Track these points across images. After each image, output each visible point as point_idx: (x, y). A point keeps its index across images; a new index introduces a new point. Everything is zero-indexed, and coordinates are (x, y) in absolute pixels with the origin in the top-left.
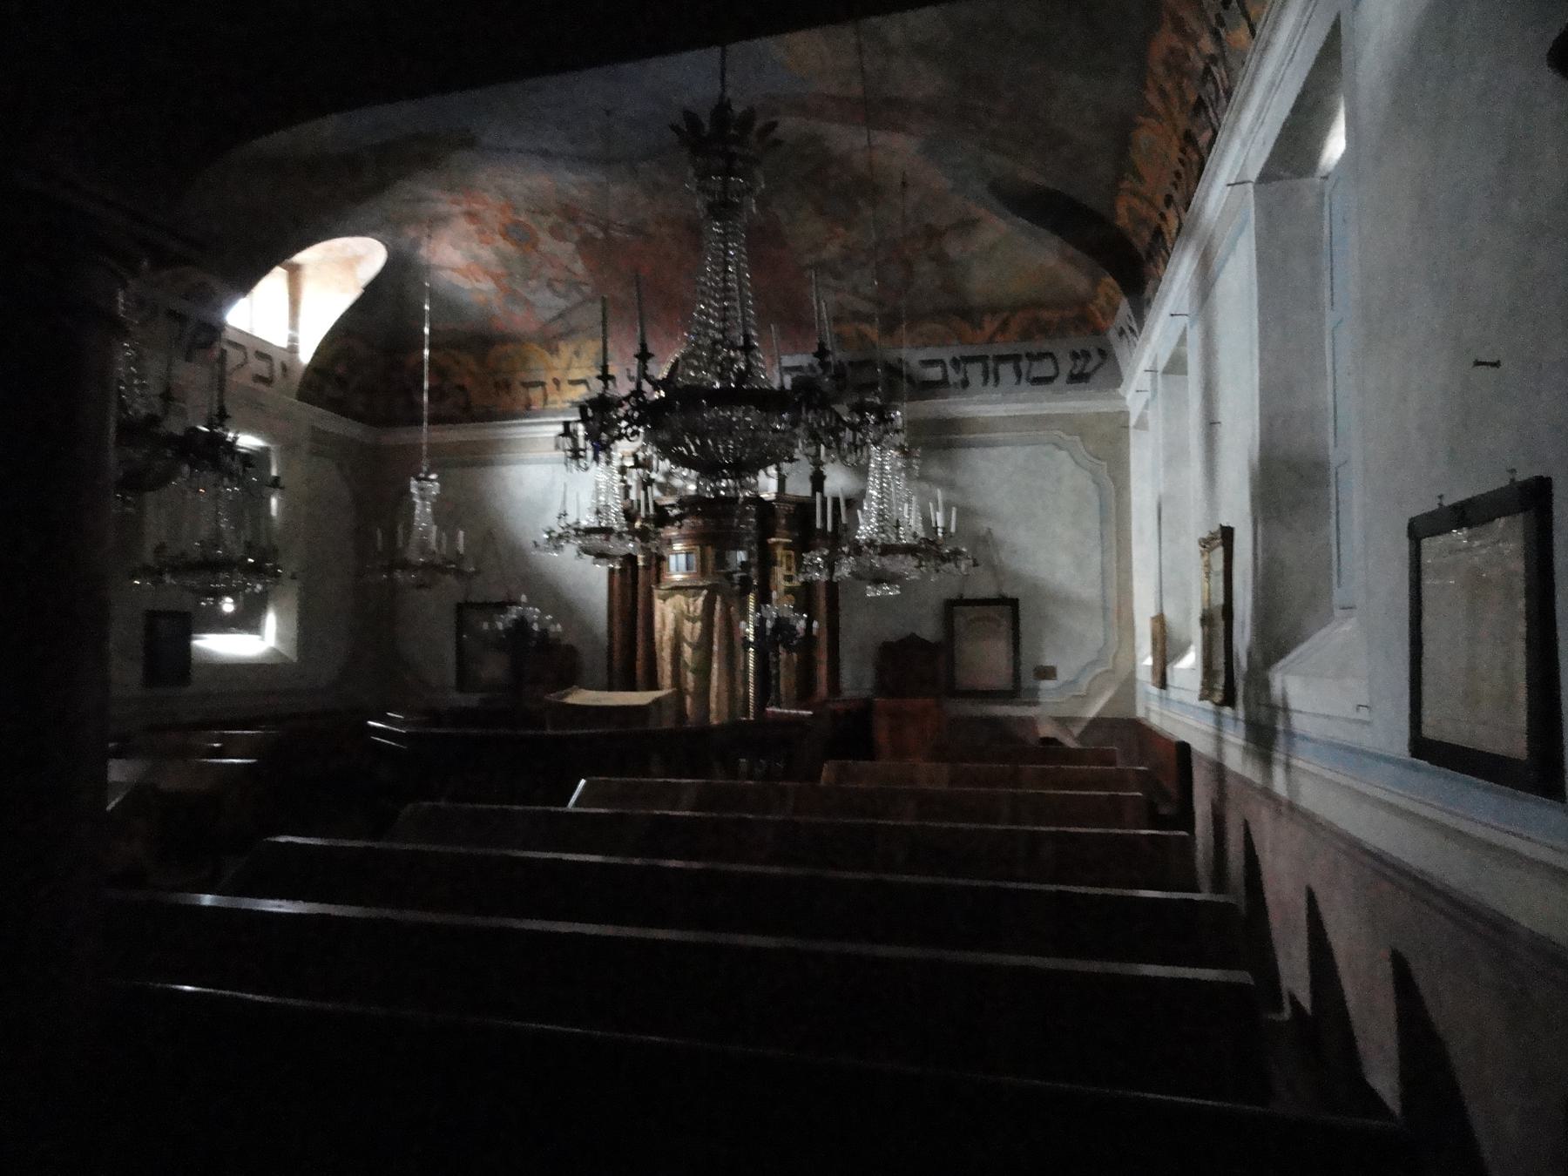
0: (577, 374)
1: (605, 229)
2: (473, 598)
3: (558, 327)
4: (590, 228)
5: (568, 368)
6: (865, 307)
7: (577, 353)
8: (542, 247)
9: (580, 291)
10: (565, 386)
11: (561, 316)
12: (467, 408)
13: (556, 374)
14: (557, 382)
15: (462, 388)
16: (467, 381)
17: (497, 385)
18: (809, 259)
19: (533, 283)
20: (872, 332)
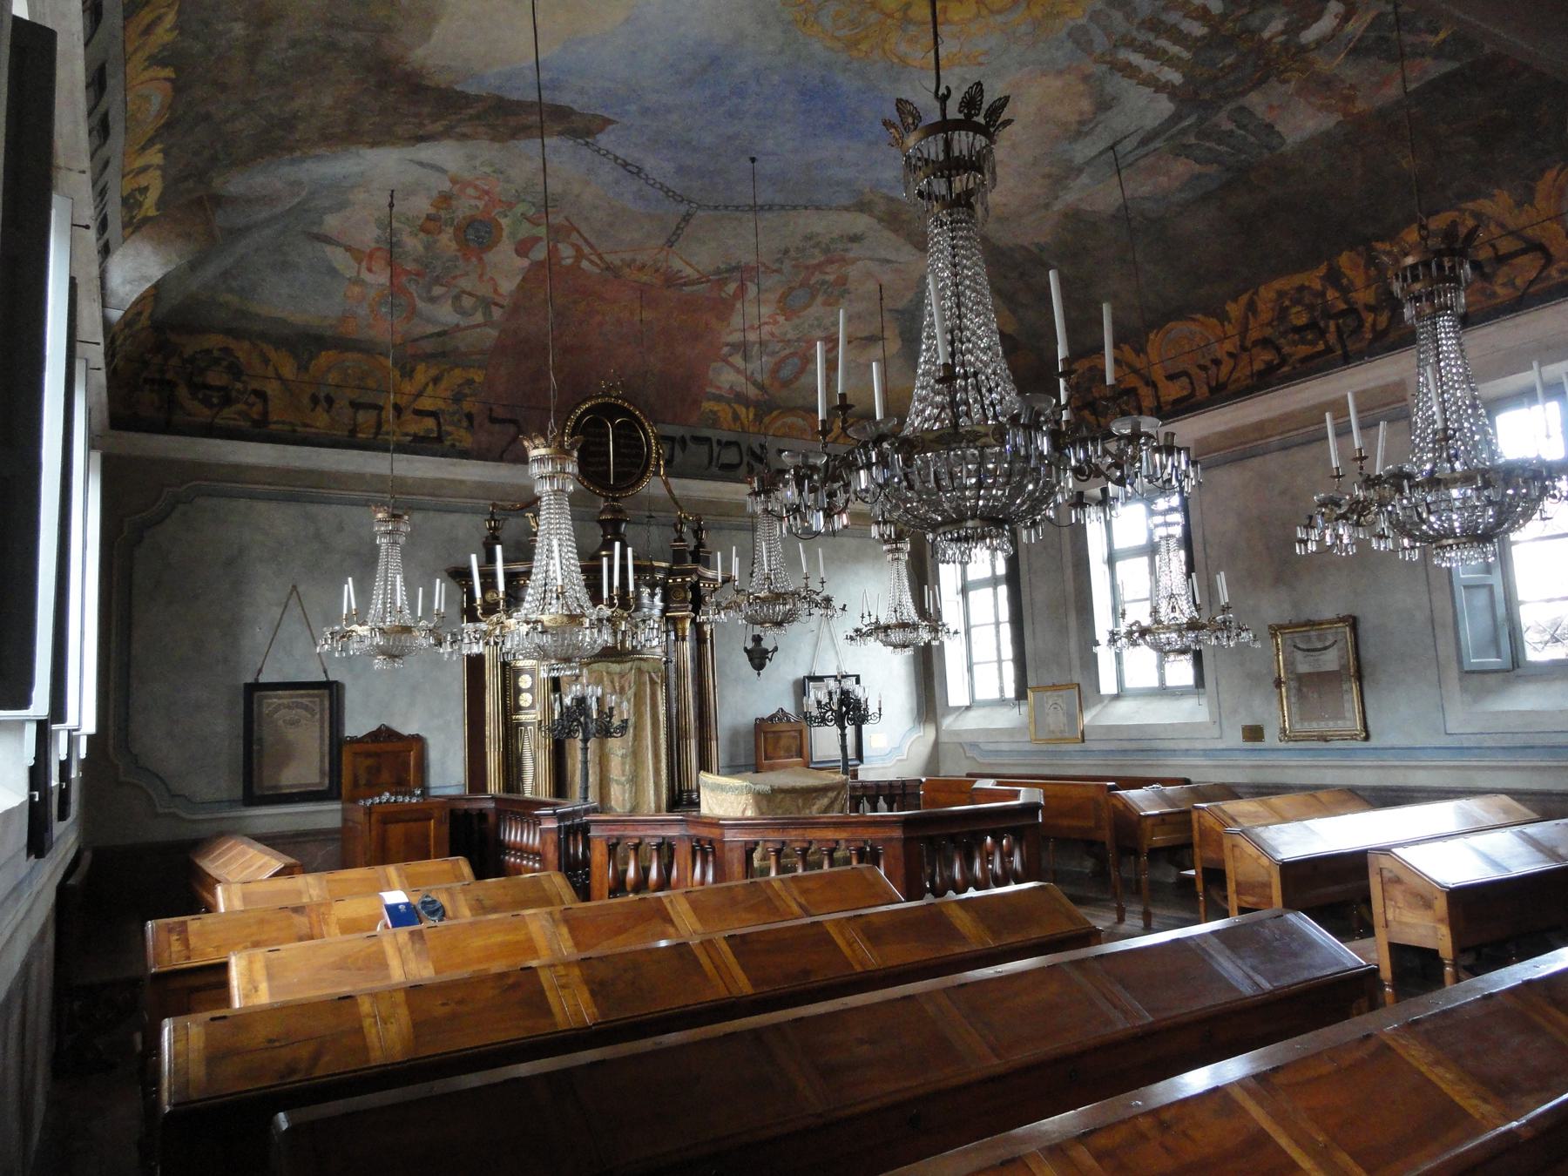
0: (426, 403)
1: (579, 255)
2: (263, 679)
3: (428, 346)
4: (566, 252)
5: (420, 394)
6: (752, 392)
7: (436, 380)
8: (490, 257)
9: (487, 314)
10: (407, 415)
11: (439, 334)
12: (263, 421)
13: (403, 401)
14: (398, 409)
15: (261, 395)
16: (272, 388)
17: (315, 400)
18: (736, 337)
19: (437, 290)
20: (747, 415)
